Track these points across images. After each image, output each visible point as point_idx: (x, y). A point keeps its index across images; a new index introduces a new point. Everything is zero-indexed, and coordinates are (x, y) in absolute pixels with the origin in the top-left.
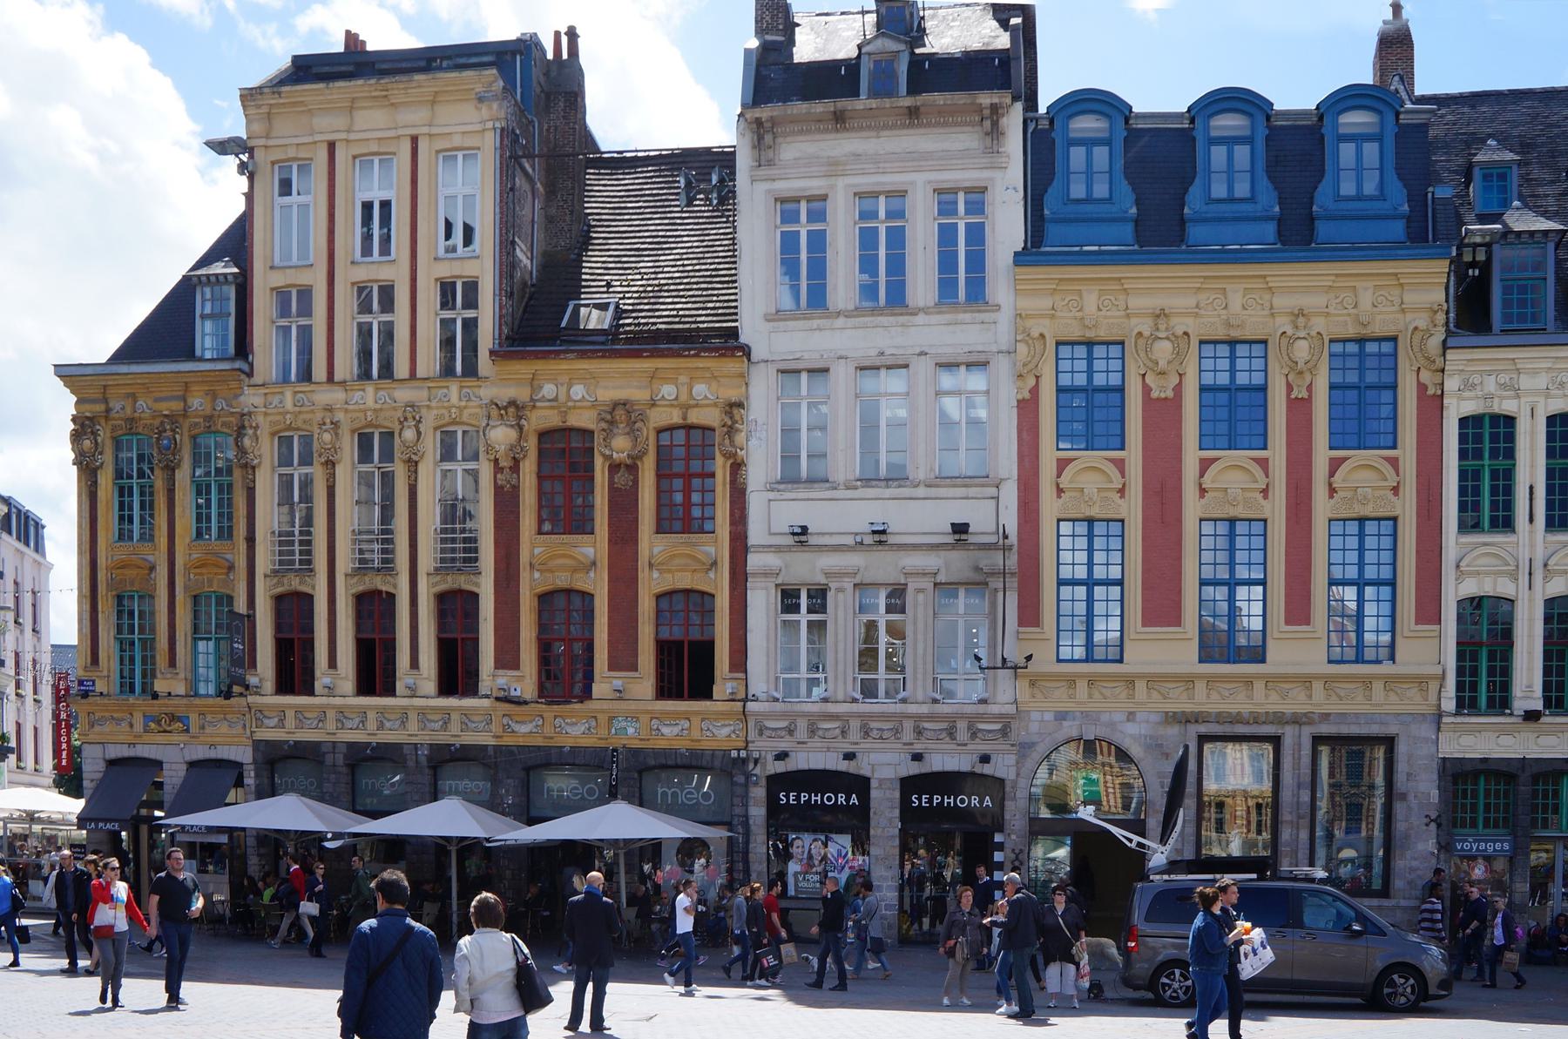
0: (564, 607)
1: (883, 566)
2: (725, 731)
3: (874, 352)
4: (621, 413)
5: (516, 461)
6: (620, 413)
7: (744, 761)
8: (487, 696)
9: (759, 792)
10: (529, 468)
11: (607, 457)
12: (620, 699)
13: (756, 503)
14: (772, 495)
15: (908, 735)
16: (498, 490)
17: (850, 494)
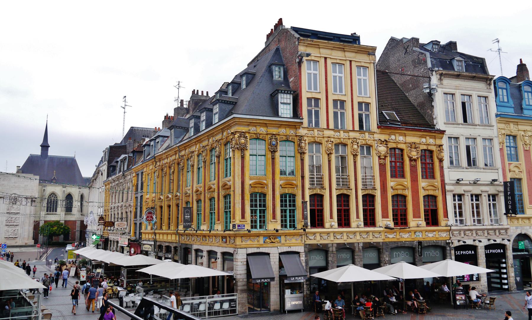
0: (400, 199)
1: (476, 190)
2: (445, 235)
3: (469, 134)
4: (413, 146)
5: (385, 157)
6: (413, 145)
7: (449, 243)
8: (380, 227)
9: (453, 252)
10: (388, 159)
11: (409, 157)
12: (418, 227)
13: (446, 171)
14: (449, 170)
15: (486, 235)
16: (380, 165)
17: (467, 170)
